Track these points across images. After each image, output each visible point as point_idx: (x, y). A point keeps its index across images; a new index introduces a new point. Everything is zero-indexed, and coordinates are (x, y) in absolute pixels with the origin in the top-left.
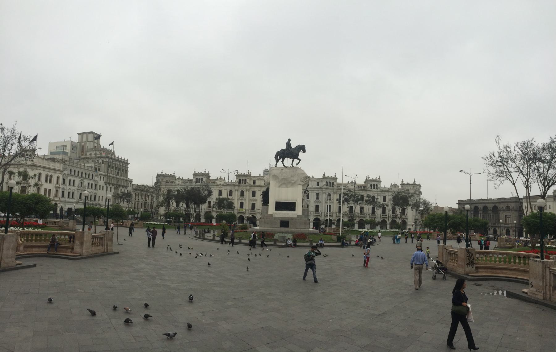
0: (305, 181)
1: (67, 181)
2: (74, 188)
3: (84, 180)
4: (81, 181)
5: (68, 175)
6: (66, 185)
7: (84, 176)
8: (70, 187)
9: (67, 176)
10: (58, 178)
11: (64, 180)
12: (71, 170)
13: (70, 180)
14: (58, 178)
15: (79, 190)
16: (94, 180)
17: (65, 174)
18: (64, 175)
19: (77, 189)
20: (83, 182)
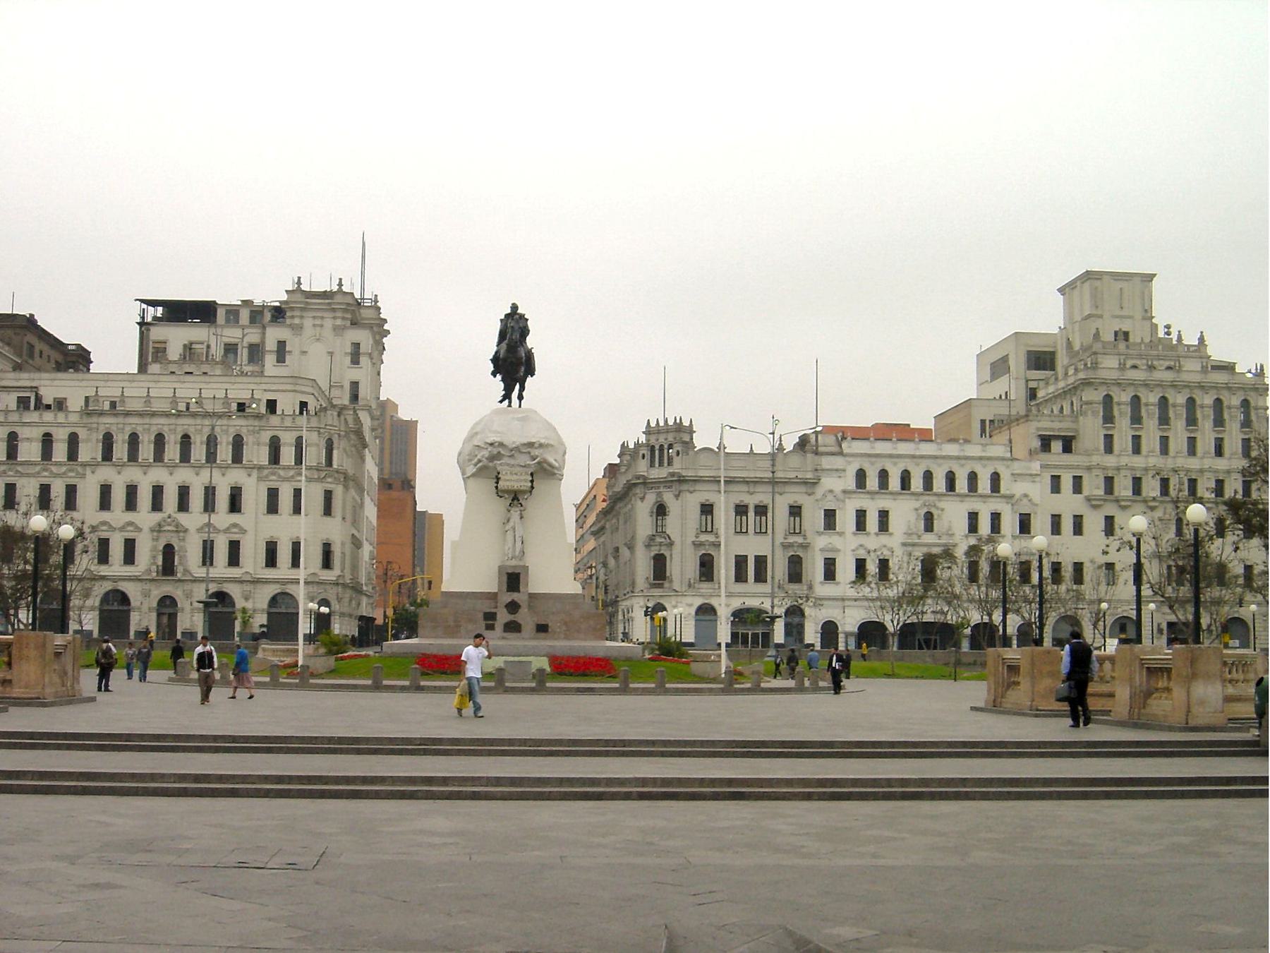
0: (476, 460)
1: (846, 520)
2: (884, 539)
3: (941, 505)
4: (925, 510)
5: (844, 492)
6: (841, 534)
7: (939, 484)
8: (861, 539)
9: (841, 496)
10: (795, 511)
11: (830, 516)
12: (861, 476)
13: (861, 516)
14: (795, 511)
15: (914, 545)
16: (1009, 497)
17: (831, 491)
18: (830, 497)
19: (904, 544)
20: (933, 510)
